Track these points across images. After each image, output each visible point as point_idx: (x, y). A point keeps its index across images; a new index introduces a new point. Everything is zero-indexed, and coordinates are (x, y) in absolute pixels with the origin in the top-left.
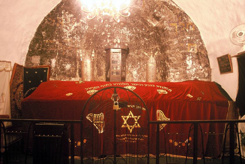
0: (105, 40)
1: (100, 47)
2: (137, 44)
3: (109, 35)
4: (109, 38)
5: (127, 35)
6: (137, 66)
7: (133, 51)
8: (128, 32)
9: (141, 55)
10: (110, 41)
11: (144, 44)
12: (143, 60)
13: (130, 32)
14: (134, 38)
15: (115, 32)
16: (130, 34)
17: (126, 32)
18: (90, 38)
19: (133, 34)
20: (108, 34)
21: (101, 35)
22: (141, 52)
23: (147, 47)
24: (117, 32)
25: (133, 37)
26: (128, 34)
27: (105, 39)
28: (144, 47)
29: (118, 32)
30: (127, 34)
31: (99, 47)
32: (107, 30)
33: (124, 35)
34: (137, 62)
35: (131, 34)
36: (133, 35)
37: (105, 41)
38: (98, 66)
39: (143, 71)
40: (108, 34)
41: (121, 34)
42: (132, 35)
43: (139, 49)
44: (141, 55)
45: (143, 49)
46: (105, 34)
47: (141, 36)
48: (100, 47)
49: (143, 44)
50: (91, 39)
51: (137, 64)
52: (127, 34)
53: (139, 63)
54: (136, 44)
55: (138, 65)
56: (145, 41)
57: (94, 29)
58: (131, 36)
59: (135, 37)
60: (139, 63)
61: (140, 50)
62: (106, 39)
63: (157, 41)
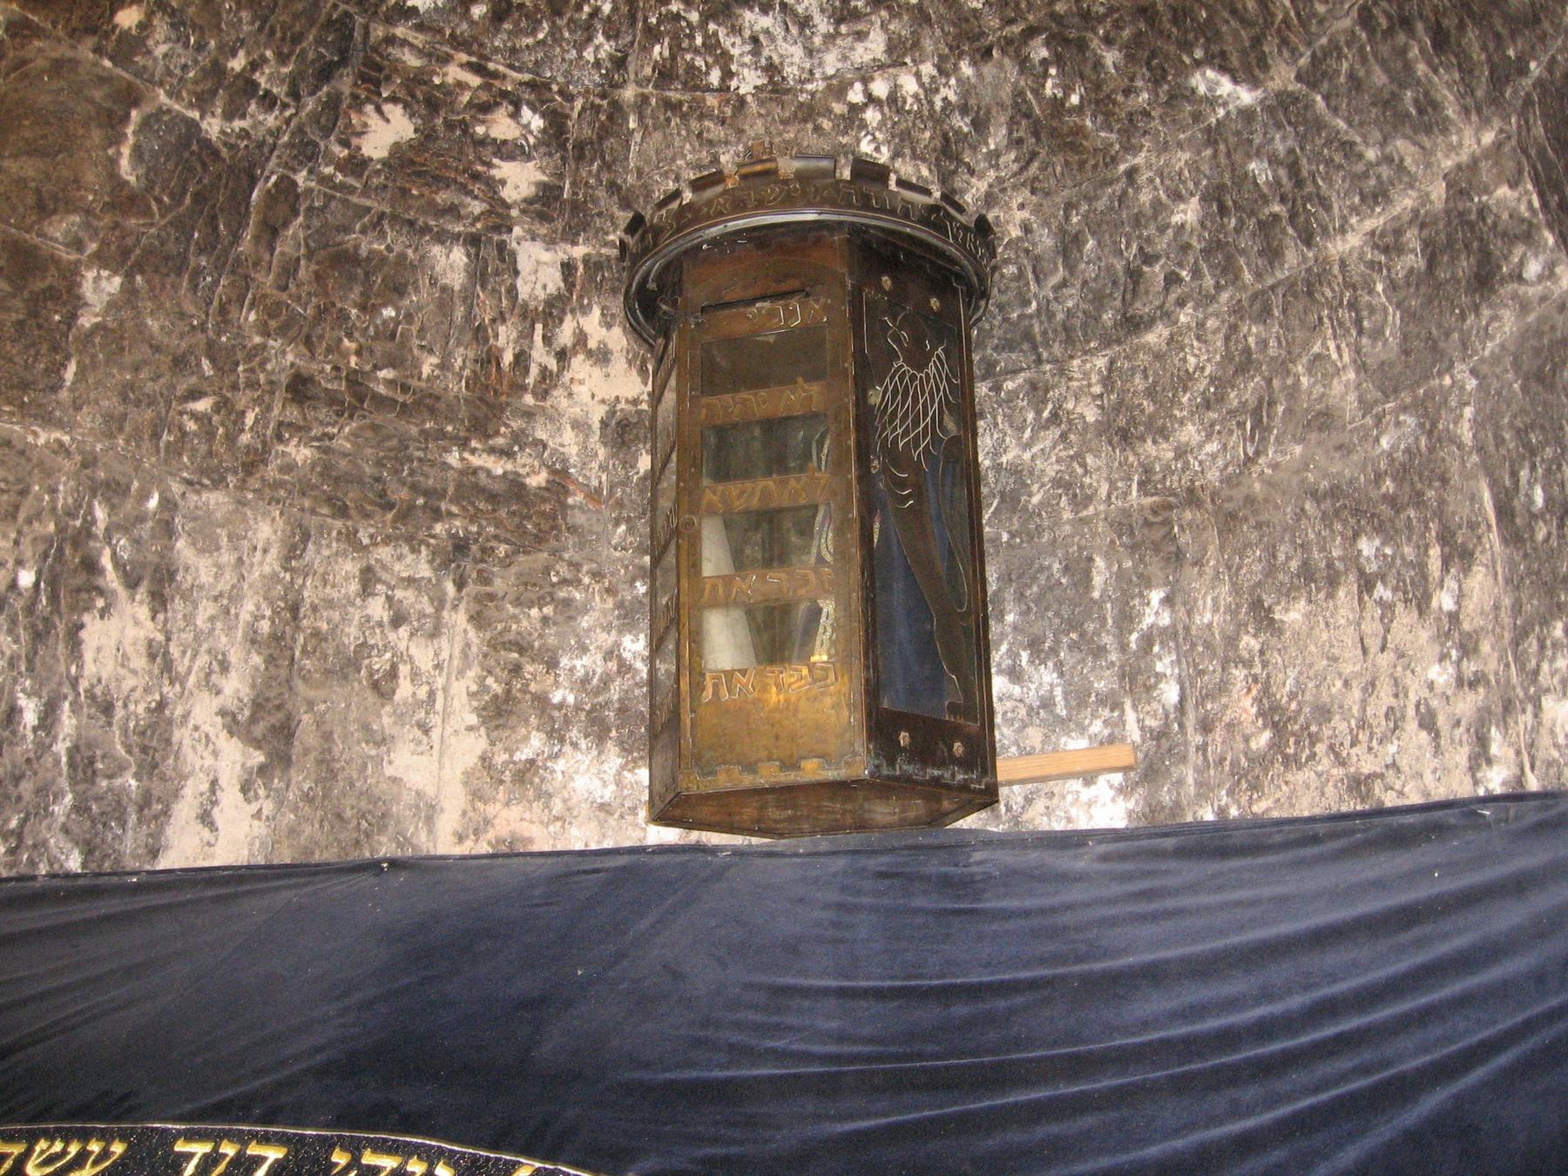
0: (459, 256)
1: (356, 382)
2: (1077, 240)
3: (509, 151)
4: (545, 203)
5: (872, 116)
6: (1137, 681)
7: (1037, 392)
8: (875, 46)
9: (1190, 433)
10: (568, 268)
11: (1215, 198)
12: (1228, 522)
13: (898, 53)
14: (997, 137)
15: (629, 93)
16: (909, 85)
17: (831, 63)
18: (44, 209)
19: (966, 69)
20: (501, 126)
21: (357, 164)
22: (1185, 380)
23: (1273, 254)
24: (665, 75)
25: (980, 125)
26: (880, 88)
27: (441, 237)
28: (1228, 270)
29: (693, 79)
30: (856, 95)
31: (321, 369)
32: (454, 73)
33: (808, 113)
34: (1121, 575)
35: (928, 69)
36: (966, 88)
37: (452, 263)
38: (285, 731)
39: (1261, 761)
40: (501, 126)
41: (742, 102)
42: (950, 93)
43: (1133, 324)
44: (1190, 433)
45: (1205, 300)
46: (427, 136)
47: (1111, 57)
48: (356, 382)
49: (1188, 213)
50: (60, 228)
51: (1127, 619)
52: (856, 95)
53: (1154, 611)
54: (1069, 245)
55: (1148, 640)
56: (1213, 136)
57: (126, 34)
58: (937, 119)
59: (1020, 111)
60: (1156, 596)
61: (1155, 337)
62: (473, 241)
63: (1441, 40)
